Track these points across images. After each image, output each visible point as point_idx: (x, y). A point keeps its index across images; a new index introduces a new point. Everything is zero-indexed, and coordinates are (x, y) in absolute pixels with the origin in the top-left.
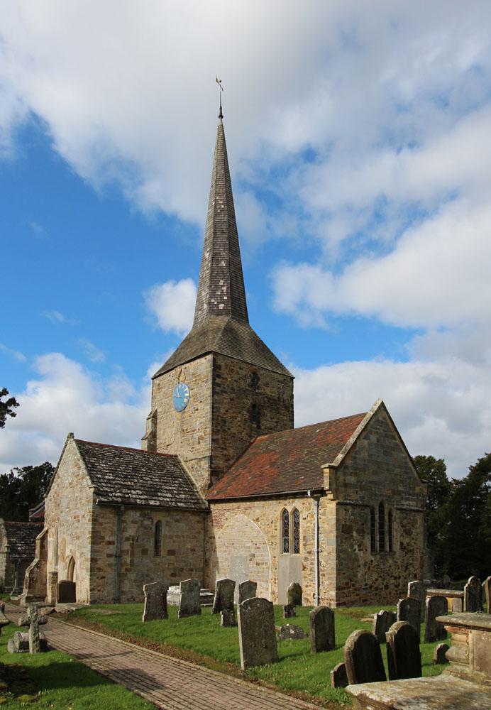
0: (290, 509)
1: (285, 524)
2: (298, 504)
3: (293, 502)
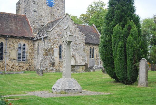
0: (92, 47)
1: (90, 51)
2: (95, 47)
3: (93, 46)
